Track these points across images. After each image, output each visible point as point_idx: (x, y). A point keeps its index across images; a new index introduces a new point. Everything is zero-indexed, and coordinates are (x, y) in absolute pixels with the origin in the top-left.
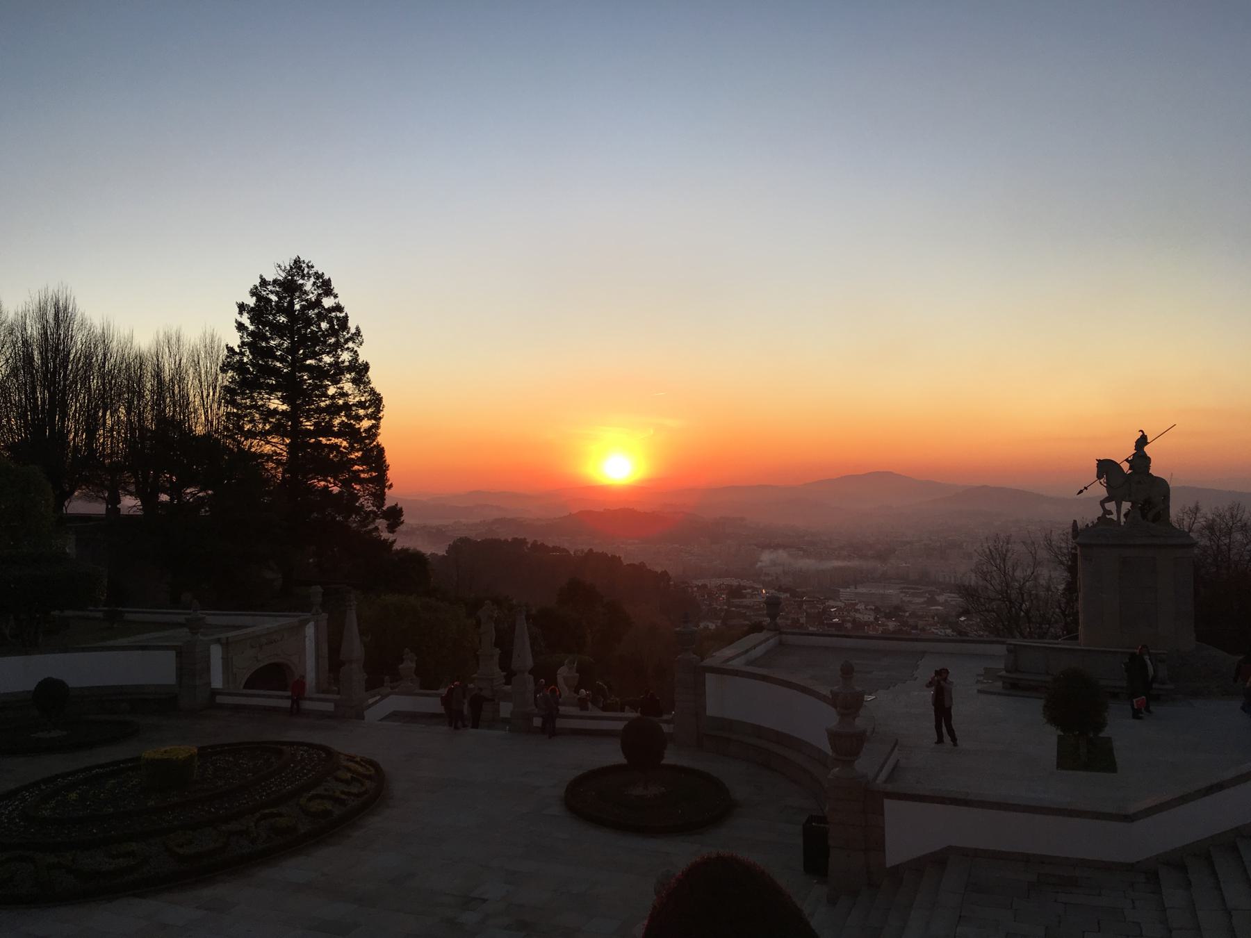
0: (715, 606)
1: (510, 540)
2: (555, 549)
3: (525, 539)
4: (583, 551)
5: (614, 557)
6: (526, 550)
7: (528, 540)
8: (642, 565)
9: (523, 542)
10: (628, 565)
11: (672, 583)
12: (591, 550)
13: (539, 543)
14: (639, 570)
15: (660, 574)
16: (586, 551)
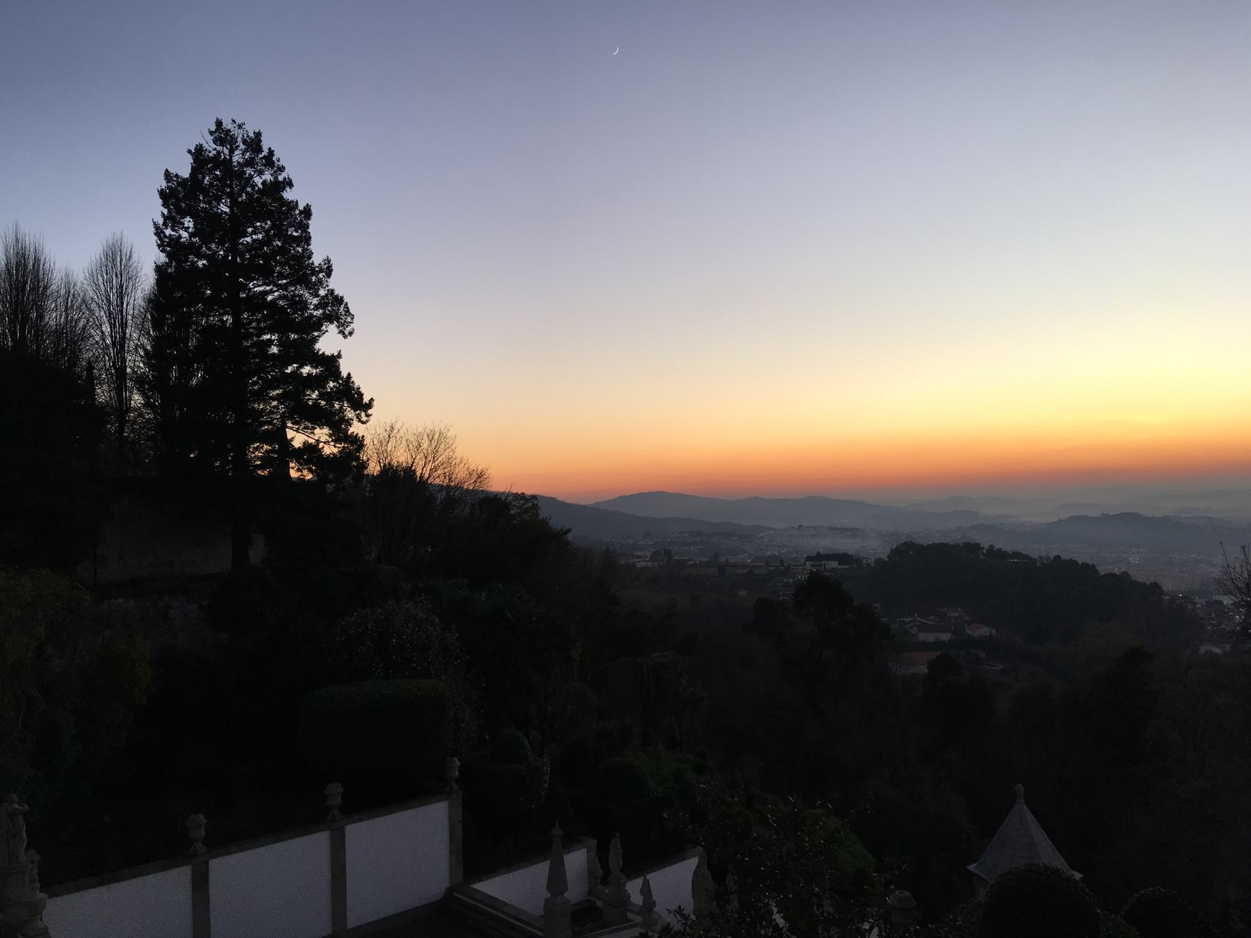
0: (1223, 626)
1: (961, 544)
2: (1016, 555)
3: (978, 545)
4: (1048, 558)
5: (1085, 565)
6: (981, 557)
7: (981, 546)
8: (1125, 575)
9: (977, 547)
10: (1105, 575)
11: (1166, 598)
12: (1057, 557)
13: (995, 549)
14: (1121, 584)
15: (1150, 585)
16: (1052, 558)
